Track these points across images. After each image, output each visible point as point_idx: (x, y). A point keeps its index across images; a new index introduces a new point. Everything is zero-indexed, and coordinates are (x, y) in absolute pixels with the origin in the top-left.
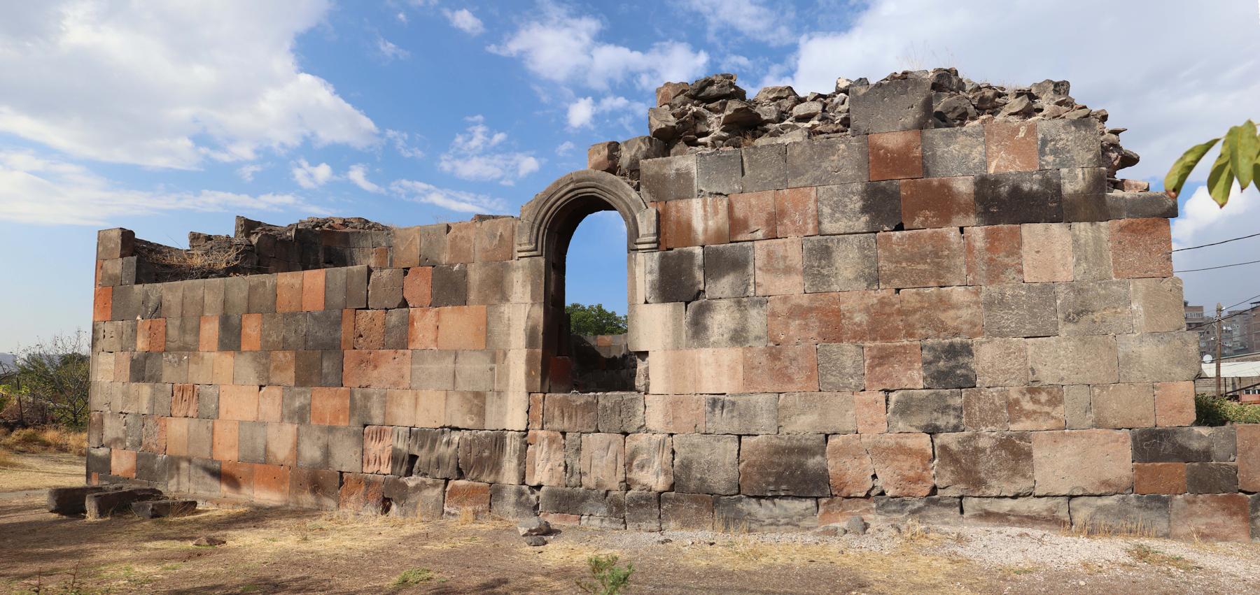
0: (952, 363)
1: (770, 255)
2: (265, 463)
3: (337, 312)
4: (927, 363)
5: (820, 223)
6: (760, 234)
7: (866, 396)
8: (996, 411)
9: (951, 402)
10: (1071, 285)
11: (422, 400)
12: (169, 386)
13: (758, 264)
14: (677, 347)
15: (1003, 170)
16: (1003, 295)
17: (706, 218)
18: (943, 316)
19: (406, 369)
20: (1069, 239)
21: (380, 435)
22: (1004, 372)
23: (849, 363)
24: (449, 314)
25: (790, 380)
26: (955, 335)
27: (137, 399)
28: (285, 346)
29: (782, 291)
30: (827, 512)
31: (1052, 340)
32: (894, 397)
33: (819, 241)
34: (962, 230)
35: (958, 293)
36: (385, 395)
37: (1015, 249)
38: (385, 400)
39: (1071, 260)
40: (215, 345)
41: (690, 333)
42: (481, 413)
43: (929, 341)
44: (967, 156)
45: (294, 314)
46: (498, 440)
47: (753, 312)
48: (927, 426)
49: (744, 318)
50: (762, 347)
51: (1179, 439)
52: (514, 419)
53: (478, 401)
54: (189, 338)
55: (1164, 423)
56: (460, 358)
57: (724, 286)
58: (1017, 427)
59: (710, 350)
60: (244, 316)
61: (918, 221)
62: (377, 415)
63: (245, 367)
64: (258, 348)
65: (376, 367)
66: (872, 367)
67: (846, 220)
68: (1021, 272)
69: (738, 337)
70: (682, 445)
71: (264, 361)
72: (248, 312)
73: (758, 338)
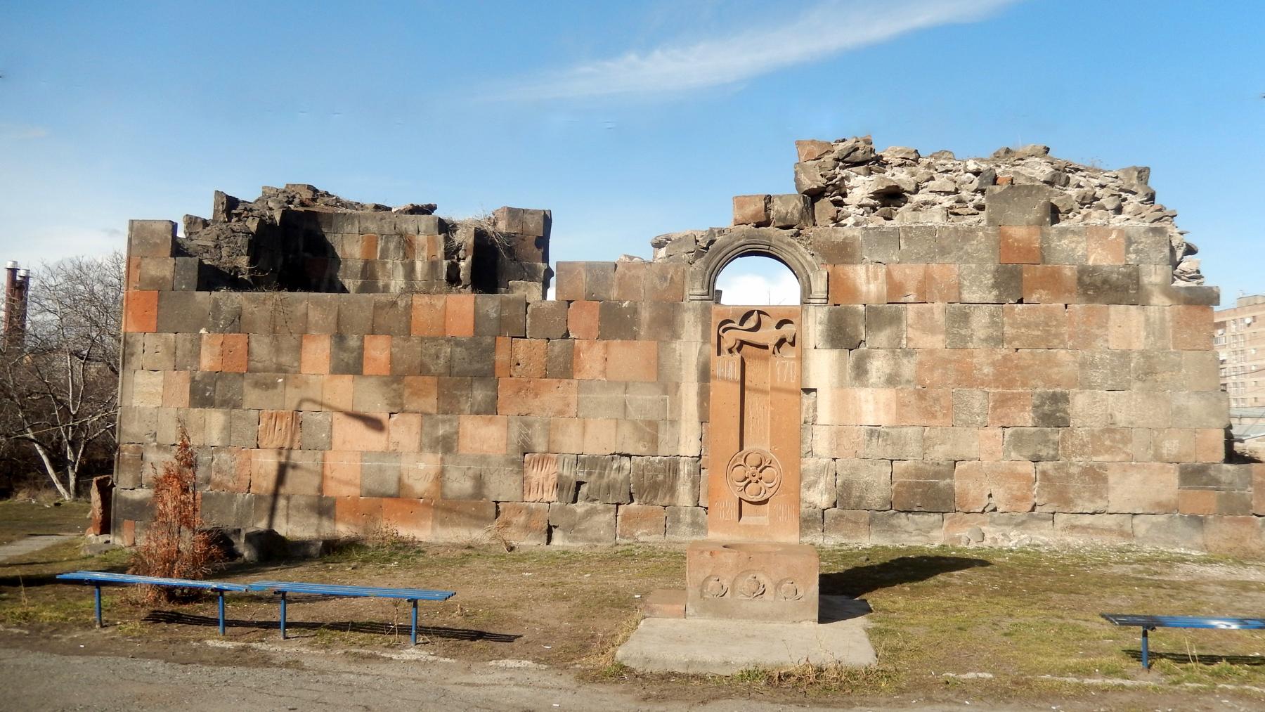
1: (920, 315)
2: (396, 496)
3: (489, 340)
5: (960, 293)
6: (911, 298)
7: (989, 431)
8: (1084, 445)
9: (1051, 437)
10: (1142, 353)
11: (591, 429)
12: (253, 414)
13: (910, 322)
14: (842, 385)
15: (1099, 263)
17: (868, 282)
19: (573, 397)
20: (1142, 318)
21: (543, 460)
22: (1091, 416)
23: (977, 405)
24: (619, 349)
25: (934, 416)
26: (1058, 385)
27: (203, 428)
28: (423, 370)
29: (929, 346)
30: (951, 524)
31: (1126, 393)
35: (1062, 354)
36: (549, 423)
37: (1103, 325)
38: (549, 428)
39: (1143, 334)
40: (326, 368)
41: (853, 375)
42: (654, 441)
43: (1038, 390)
44: (1073, 250)
45: (434, 339)
47: (905, 361)
50: (911, 389)
51: (1212, 473)
53: (651, 431)
54: (286, 359)
55: (1202, 460)
57: (882, 337)
58: (1099, 459)
59: (870, 390)
61: (1035, 297)
62: (540, 445)
65: (536, 395)
66: (994, 408)
69: (892, 380)
71: (395, 386)
72: (373, 333)
73: (908, 382)
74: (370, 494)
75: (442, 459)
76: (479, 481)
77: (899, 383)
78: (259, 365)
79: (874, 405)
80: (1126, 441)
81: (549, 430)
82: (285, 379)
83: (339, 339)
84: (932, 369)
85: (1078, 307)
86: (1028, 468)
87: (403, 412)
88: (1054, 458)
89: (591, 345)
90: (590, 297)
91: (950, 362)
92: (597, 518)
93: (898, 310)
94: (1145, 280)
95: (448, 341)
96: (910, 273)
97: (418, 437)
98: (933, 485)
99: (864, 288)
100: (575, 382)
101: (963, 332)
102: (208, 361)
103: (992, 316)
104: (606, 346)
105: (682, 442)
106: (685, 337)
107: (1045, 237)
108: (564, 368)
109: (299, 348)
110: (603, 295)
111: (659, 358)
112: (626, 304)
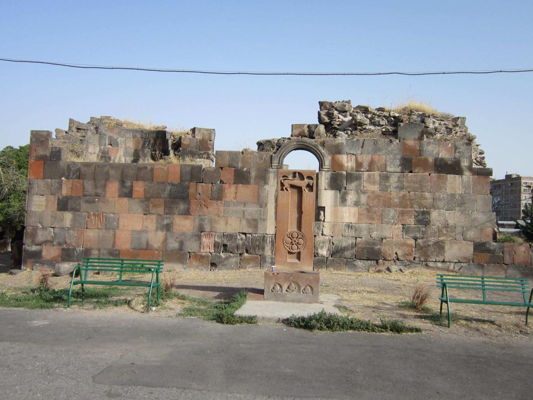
0: (423, 217)
1: (369, 176)
2: (147, 249)
4: (416, 216)
5: (386, 168)
7: (397, 226)
8: (435, 233)
10: (460, 195)
11: (229, 222)
13: (365, 179)
14: (335, 206)
15: (443, 157)
16: (440, 196)
17: (348, 162)
18: (422, 202)
19: (222, 209)
21: (209, 235)
25: (374, 219)
27: (62, 220)
29: (372, 189)
33: (386, 175)
34: (430, 174)
36: (211, 219)
38: (211, 221)
40: (117, 195)
42: (256, 227)
45: (163, 183)
46: (264, 238)
47: (362, 196)
48: (414, 237)
49: (359, 197)
53: (254, 223)
54: (99, 191)
57: (352, 186)
59: (347, 208)
60: (134, 182)
61: (417, 170)
62: (207, 228)
63: (136, 206)
66: (398, 216)
67: (394, 167)
68: (446, 189)
69: (357, 204)
71: (146, 203)
73: (363, 204)
75: (166, 234)
76: (182, 244)
77: (359, 205)
78: (87, 193)
79: (349, 214)
80: (452, 231)
81: (211, 222)
82: (99, 199)
83: (122, 182)
84: (373, 200)
85: (433, 175)
86: (412, 242)
88: (422, 238)
89: (230, 187)
91: (381, 196)
94: (462, 164)
95: (169, 184)
96: (365, 159)
98: (372, 248)
99: (346, 165)
101: (387, 184)
102: (65, 192)
103: (399, 178)
104: (237, 187)
105: (268, 228)
107: (421, 146)
108: (219, 196)
109: (105, 186)
110: (235, 165)
111: (258, 193)
112: (245, 169)
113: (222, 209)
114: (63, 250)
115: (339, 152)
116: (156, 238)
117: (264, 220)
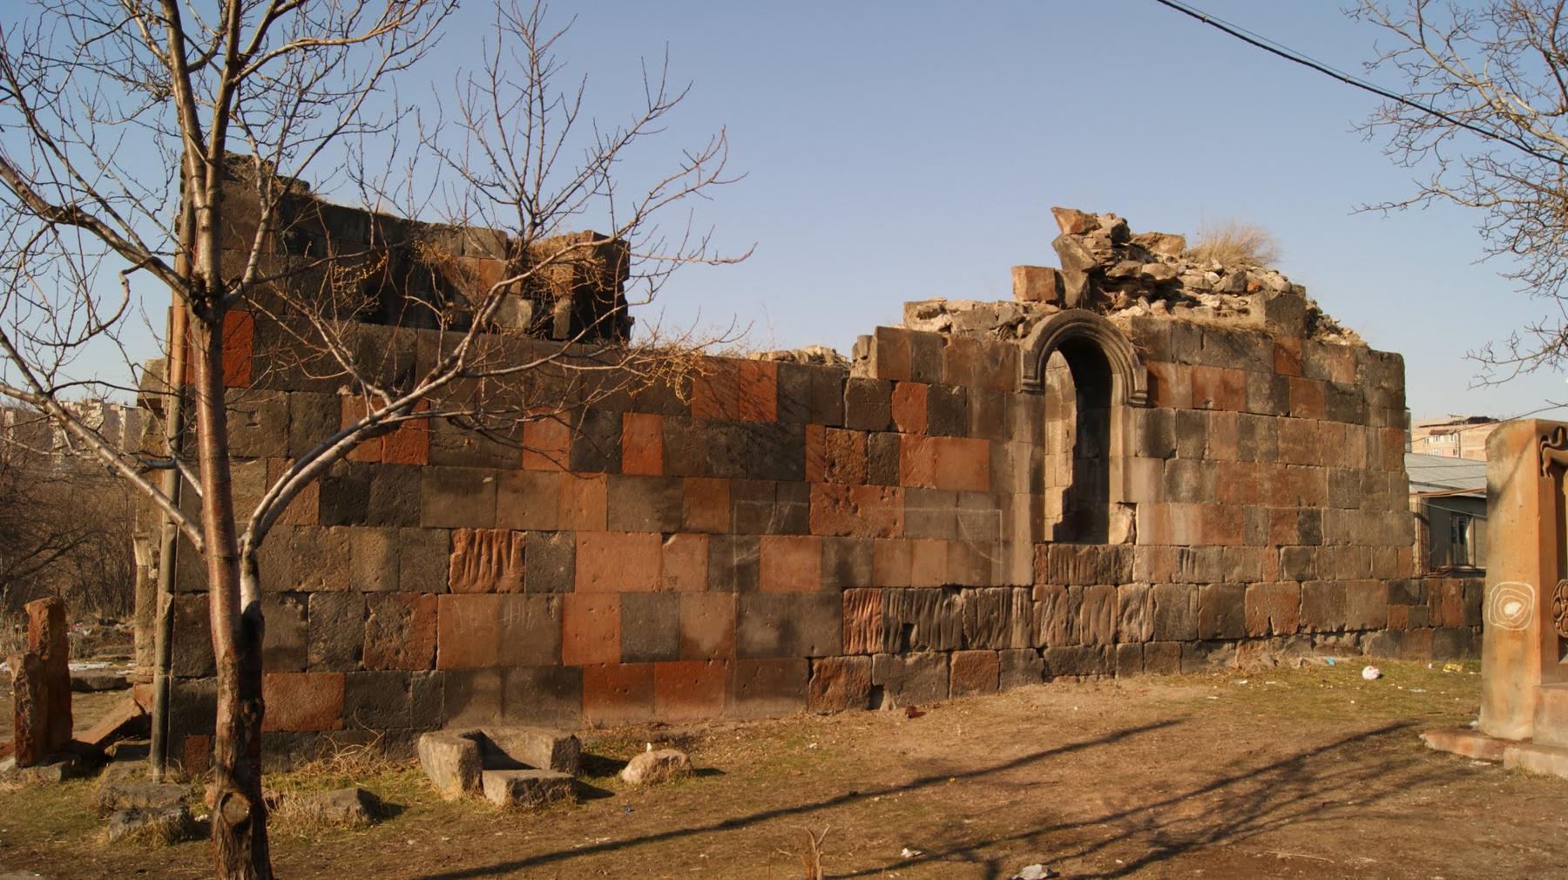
2: (674, 657)
14: (1157, 502)
19: (900, 511)
25: (1230, 536)
32: (1282, 550)
42: (987, 567)
52: (1022, 574)
56: (962, 500)
62: (861, 573)
64: (657, 471)
69: (1197, 495)
70: (1160, 594)
74: (631, 658)
75: (738, 600)
76: (787, 630)
79: (1184, 525)
81: (872, 556)
82: (497, 477)
87: (682, 530)
90: (917, 378)
92: (929, 671)
93: (1201, 417)
96: (1210, 376)
97: (704, 569)
100: (900, 492)
101: (1249, 444)
104: (936, 444)
106: (1016, 437)
113: (900, 511)
114: (349, 684)
115: (1161, 357)
116: (706, 621)
117: (1008, 544)
